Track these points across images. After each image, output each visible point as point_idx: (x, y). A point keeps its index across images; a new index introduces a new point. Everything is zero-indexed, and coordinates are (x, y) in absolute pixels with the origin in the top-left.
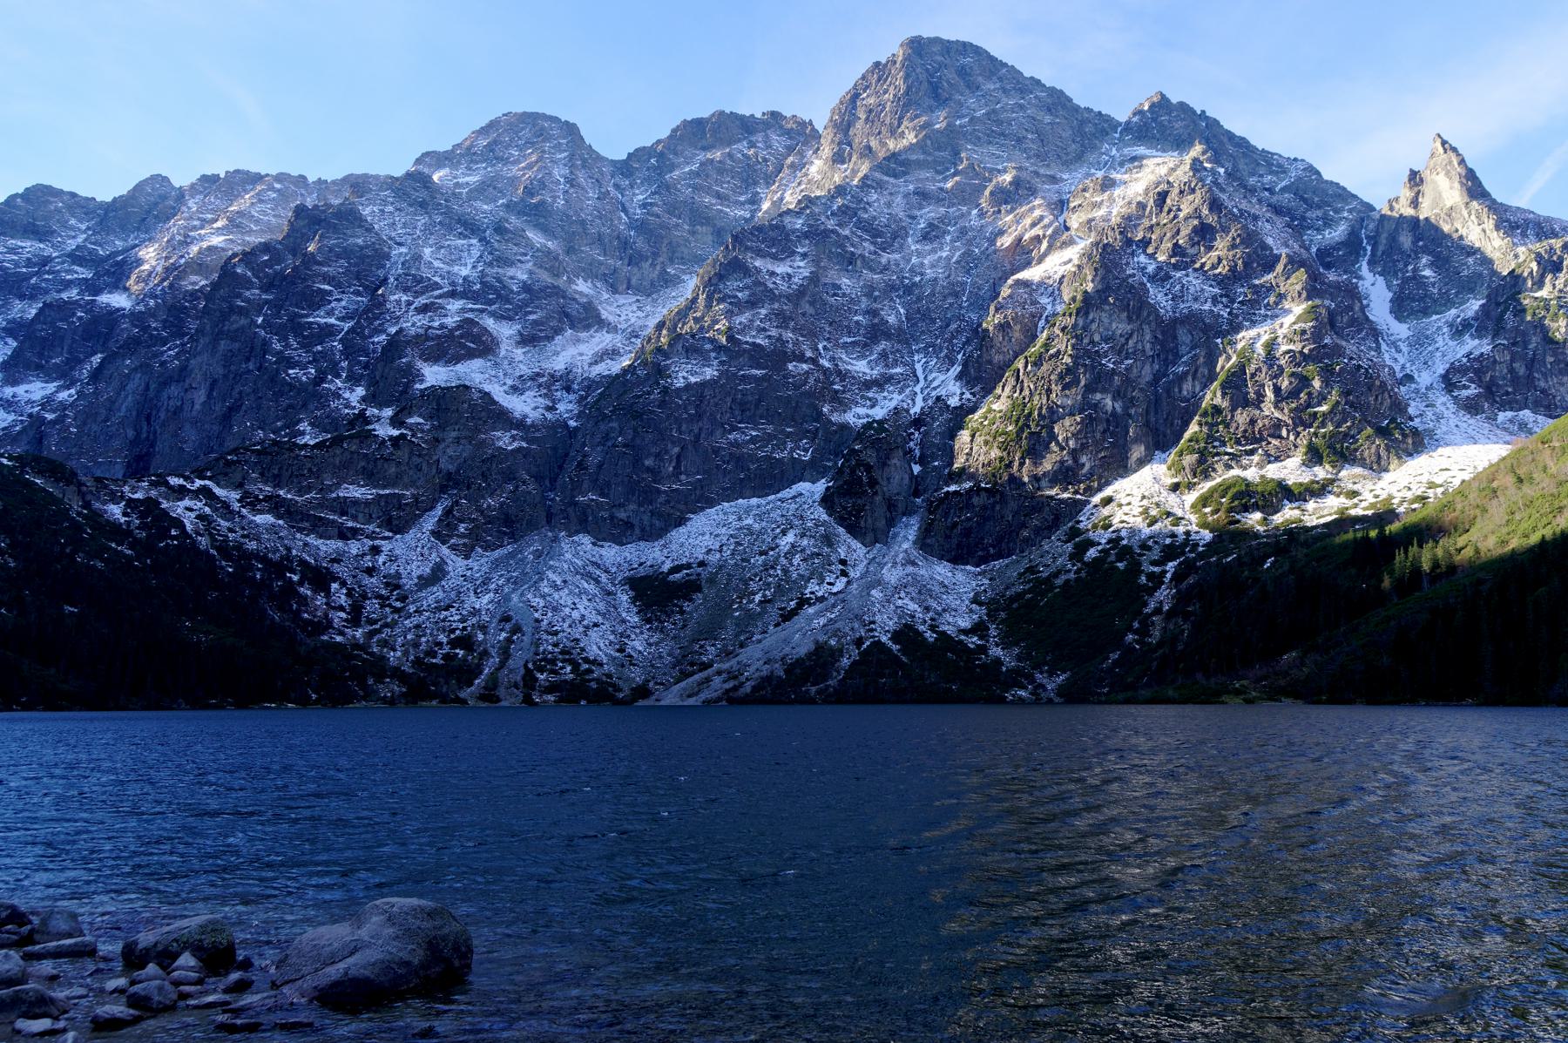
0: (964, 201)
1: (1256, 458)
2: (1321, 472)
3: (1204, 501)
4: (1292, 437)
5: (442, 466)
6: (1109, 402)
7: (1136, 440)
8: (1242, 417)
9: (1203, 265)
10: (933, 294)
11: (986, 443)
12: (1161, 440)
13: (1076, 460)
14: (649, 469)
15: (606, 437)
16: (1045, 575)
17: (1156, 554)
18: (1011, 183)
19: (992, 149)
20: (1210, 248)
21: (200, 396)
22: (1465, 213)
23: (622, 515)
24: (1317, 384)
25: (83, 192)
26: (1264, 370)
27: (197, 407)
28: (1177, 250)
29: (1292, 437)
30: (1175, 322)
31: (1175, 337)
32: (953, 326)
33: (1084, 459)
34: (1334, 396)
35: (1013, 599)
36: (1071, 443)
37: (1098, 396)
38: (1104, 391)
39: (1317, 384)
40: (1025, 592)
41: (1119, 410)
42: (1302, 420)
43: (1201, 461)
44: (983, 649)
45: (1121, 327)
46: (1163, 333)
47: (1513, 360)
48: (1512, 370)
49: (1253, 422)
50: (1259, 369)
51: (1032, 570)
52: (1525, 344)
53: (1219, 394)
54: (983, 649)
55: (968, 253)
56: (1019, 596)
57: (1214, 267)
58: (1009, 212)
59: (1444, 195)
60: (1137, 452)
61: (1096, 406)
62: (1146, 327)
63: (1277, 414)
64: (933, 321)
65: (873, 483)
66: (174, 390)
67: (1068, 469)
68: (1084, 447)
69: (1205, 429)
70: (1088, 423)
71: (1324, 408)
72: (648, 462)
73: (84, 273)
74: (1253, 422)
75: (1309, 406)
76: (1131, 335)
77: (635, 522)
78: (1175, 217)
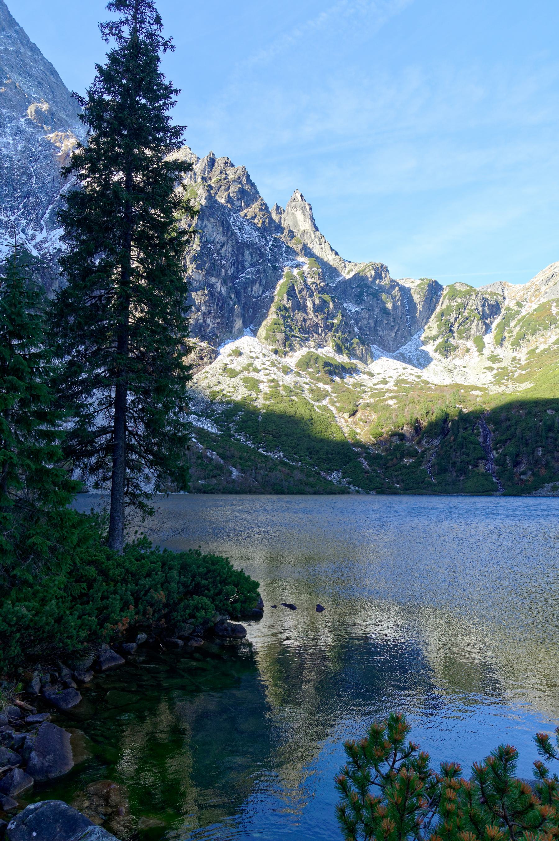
0: (12, 108)
1: (312, 344)
2: (343, 359)
4: (323, 335)
6: (218, 284)
7: (237, 316)
8: (299, 316)
9: (246, 215)
10: (11, 167)
12: (252, 320)
13: (204, 321)
18: (48, 111)
19: (24, 80)
20: (248, 206)
22: (313, 236)
24: (331, 306)
26: (305, 290)
28: (229, 199)
29: (323, 335)
30: (244, 243)
31: (243, 255)
32: (33, 199)
33: (209, 321)
34: (339, 317)
36: (203, 308)
37: (213, 280)
38: (217, 277)
39: (331, 306)
41: (224, 293)
42: (329, 327)
43: (287, 338)
45: (220, 238)
46: (238, 250)
47: (369, 319)
48: (368, 323)
49: (305, 321)
50: (302, 289)
52: (373, 311)
53: (285, 298)
55: (26, 149)
57: (254, 218)
58: (52, 132)
59: (300, 223)
60: (238, 324)
61: (212, 286)
62: (230, 242)
63: (315, 319)
64: (15, 189)
67: (201, 326)
68: (209, 312)
69: (281, 319)
70: (211, 295)
71: (335, 321)
74: (305, 321)
75: (327, 318)
76: (224, 244)
78: (226, 178)
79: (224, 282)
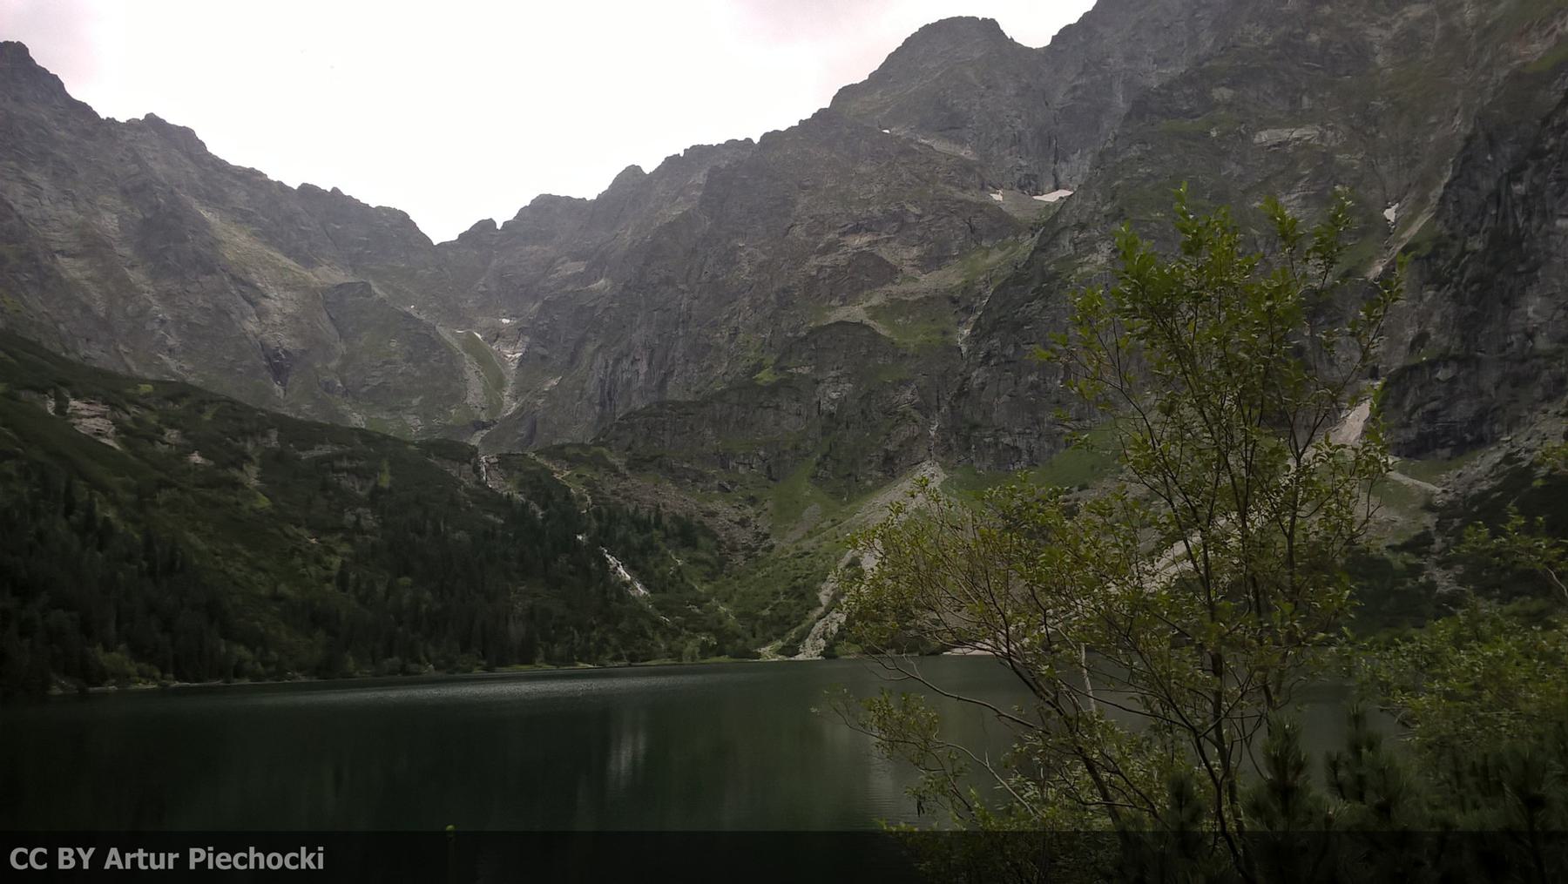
5: (823, 407)
11: (1454, 296)
14: (1033, 386)
15: (988, 356)
16: (1525, 464)
21: (643, 367)
23: (1007, 440)
25: (576, 195)
27: (642, 377)
35: (1476, 500)
40: (1494, 489)
44: (1416, 571)
51: (1508, 458)
54: (1416, 571)
56: (1484, 495)
66: (625, 364)
72: (1030, 378)
73: (581, 267)
77: (1021, 444)
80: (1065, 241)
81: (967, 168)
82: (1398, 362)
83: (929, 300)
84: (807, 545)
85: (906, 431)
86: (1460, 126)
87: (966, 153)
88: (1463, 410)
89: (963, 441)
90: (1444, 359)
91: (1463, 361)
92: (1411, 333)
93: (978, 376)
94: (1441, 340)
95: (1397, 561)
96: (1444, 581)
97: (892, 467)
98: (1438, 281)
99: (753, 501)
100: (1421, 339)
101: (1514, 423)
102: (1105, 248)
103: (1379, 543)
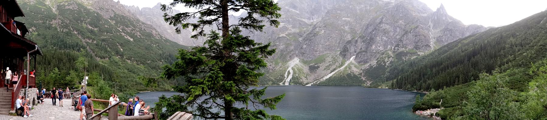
3: (397, 54)
17: (389, 63)
54: (360, 77)
65: (348, 50)
79: (387, 37)
80: (317, 29)
81: (298, 14)
82: (358, 51)
83: (294, 33)
84: (281, 69)
85: (292, 53)
86: (367, 23)
87: (298, 12)
88: (366, 58)
89: (302, 54)
90: (364, 51)
91: (366, 52)
92: (360, 48)
93: (305, 46)
94: (363, 49)
95: (359, 76)
96: (364, 79)
97: (291, 58)
98: (363, 42)
99: (272, 62)
100: (361, 49)
101: (370, 60)
102: (323, 31)
103: (357, 74)
